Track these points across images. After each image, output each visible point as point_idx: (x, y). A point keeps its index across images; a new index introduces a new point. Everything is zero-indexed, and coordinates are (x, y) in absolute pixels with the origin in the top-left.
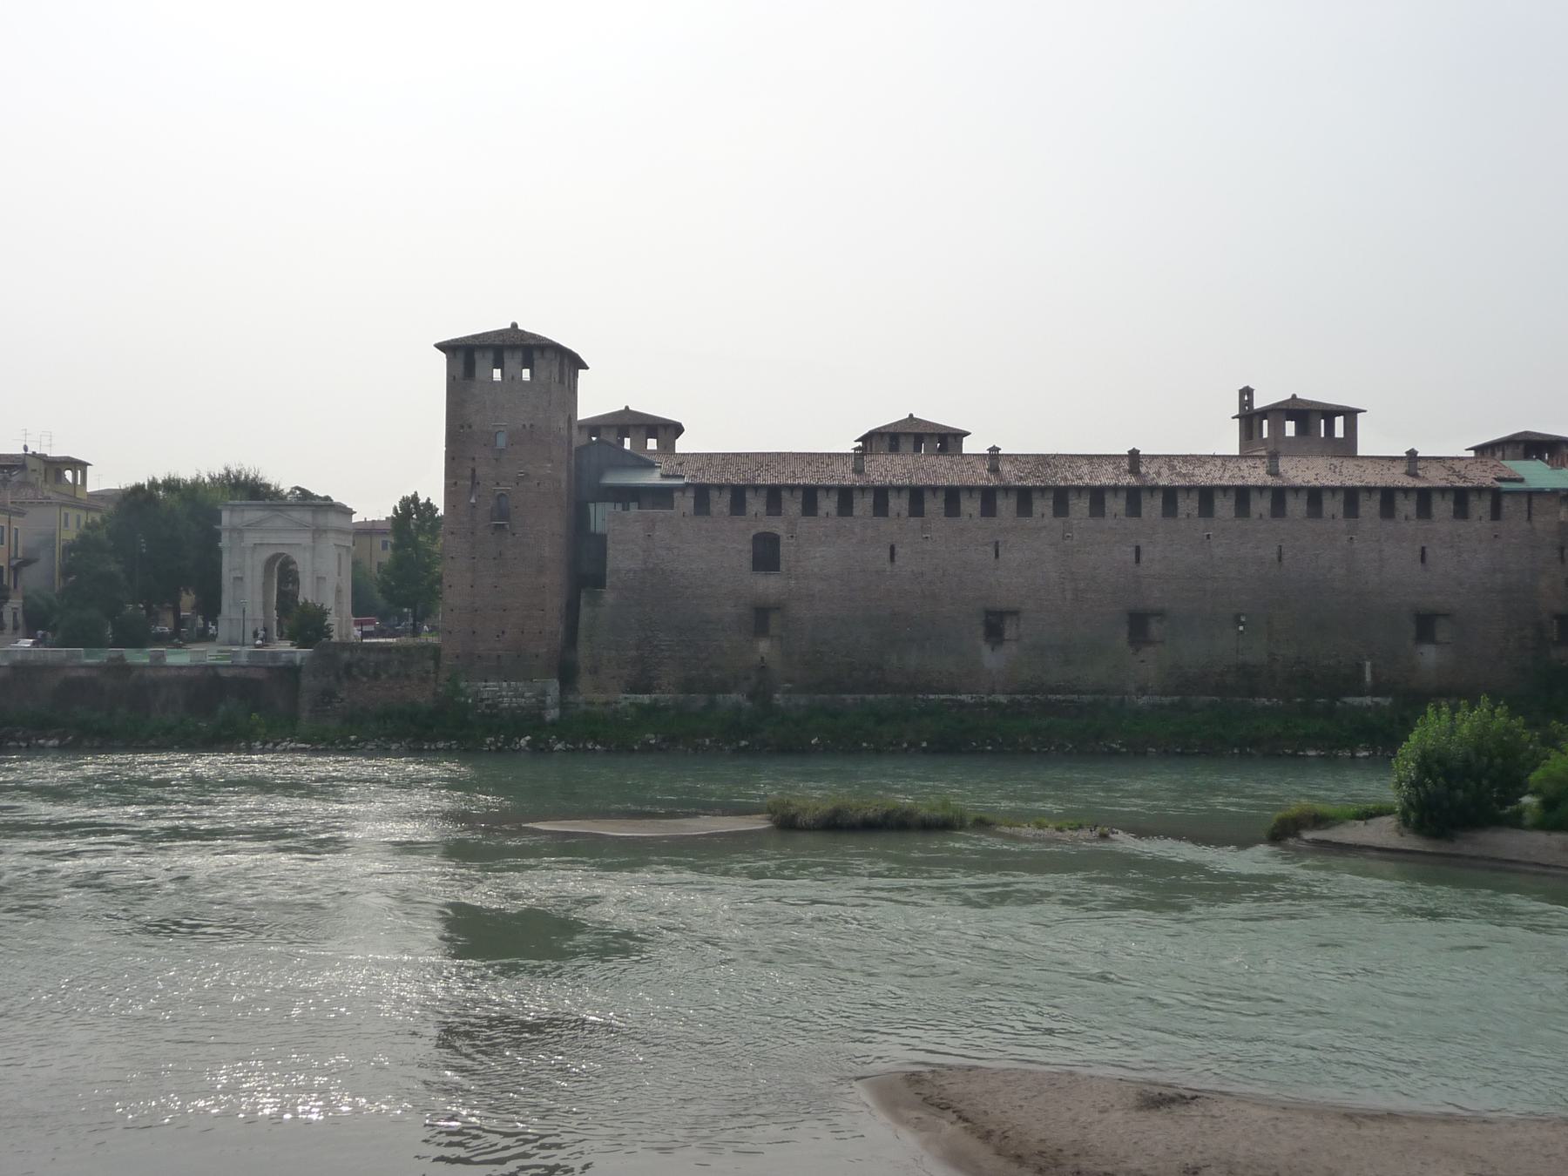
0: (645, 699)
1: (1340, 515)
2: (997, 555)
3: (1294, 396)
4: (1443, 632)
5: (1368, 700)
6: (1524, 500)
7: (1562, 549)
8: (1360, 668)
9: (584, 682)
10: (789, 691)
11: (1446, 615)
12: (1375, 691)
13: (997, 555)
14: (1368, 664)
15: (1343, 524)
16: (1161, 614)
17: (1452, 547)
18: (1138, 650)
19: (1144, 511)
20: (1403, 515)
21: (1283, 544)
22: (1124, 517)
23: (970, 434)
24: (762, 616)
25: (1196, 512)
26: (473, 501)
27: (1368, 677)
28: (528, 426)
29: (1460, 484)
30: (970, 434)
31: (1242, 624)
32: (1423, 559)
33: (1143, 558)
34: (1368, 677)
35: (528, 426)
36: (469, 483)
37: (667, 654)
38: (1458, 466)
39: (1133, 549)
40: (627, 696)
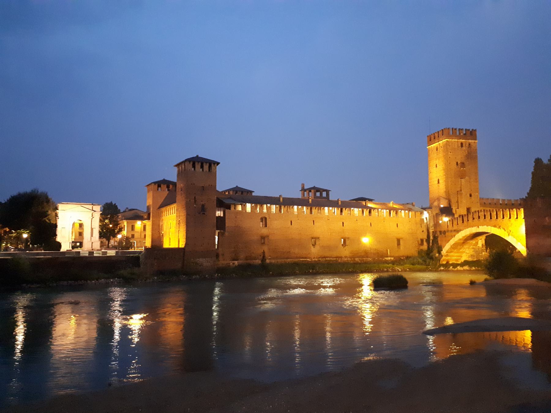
0: (236, 263)
2: (314, 224)
5: (389, 258)
8: (387, 250)
9: (221, 258)
10: (270, 259)
13: (314, 224)
14: (389, 250)
16: (348, 238)
23: (254, 192)
24: (263, 239)
26: (195, 206)
28: (210, 185)
30: (254, 192)
32: (397, 227)
35: (210, 185)
36: (194, 201)
37: (241, 250)
39: (342, 223)
40: (232, 261)
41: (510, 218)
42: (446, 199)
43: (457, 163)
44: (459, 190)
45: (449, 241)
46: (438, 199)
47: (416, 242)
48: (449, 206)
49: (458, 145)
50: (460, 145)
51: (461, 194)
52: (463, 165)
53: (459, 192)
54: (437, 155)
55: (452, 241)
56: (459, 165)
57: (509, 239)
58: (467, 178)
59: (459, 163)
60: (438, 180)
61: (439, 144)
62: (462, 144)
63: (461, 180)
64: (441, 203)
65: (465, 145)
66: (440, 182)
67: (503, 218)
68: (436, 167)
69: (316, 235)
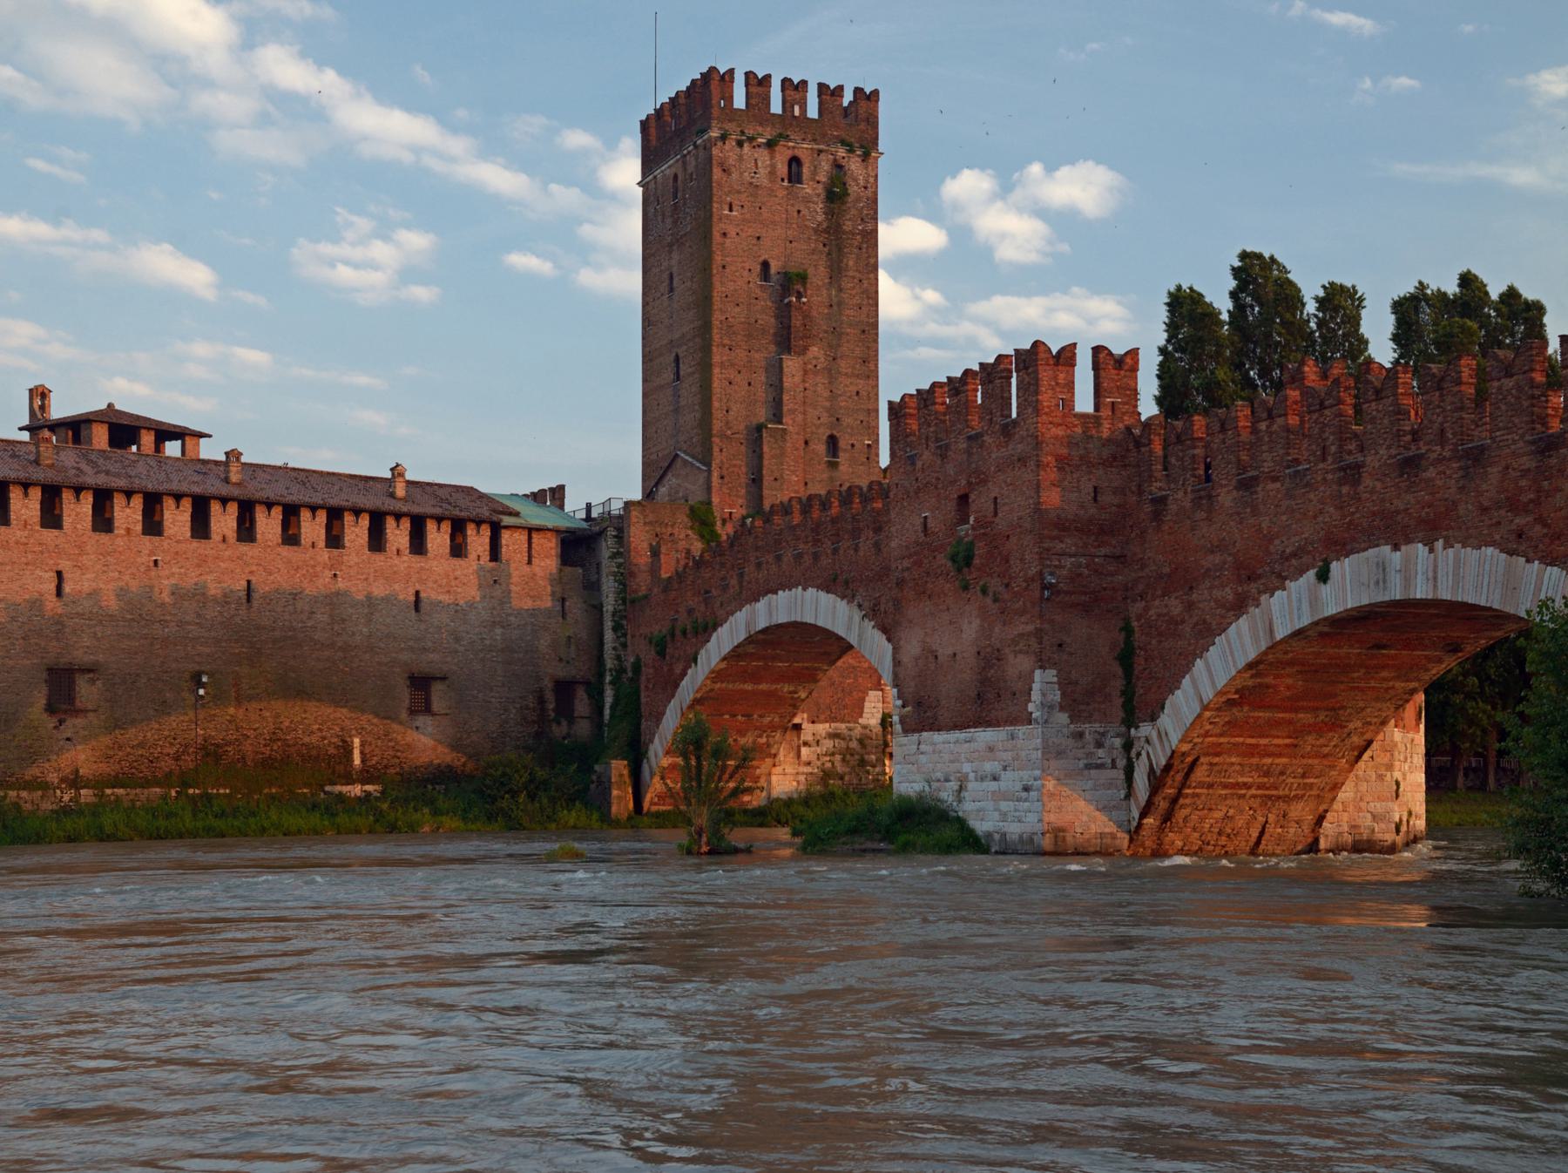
1: (322, 544)
3: (110, 406)
4: (439, 697)
6: (524, 537)
7: (563, 600)
11: (443, 679)
12: (366, 776)
14: (357, 741)
15: (325, 555)
17: (449, 592)
18: (61, 722)
19: (67, 521)
20: (394, 549)
21: (253, 579)
22: (38, 528)
25: (139, 528)
27: (357, 761)
29: (457, 512)
31: (200, 684)
33: (67, 588)
34: (357, 761)
38: (440, 492)
43: (765, 265)
47: (531, 701)
49: (773, 166)
50: (782, 169)
54: (675, 222)
56: (774, 278)
58: (814, 350)
59: (773, 270)
65: (814, 172)
68: (671, 290)
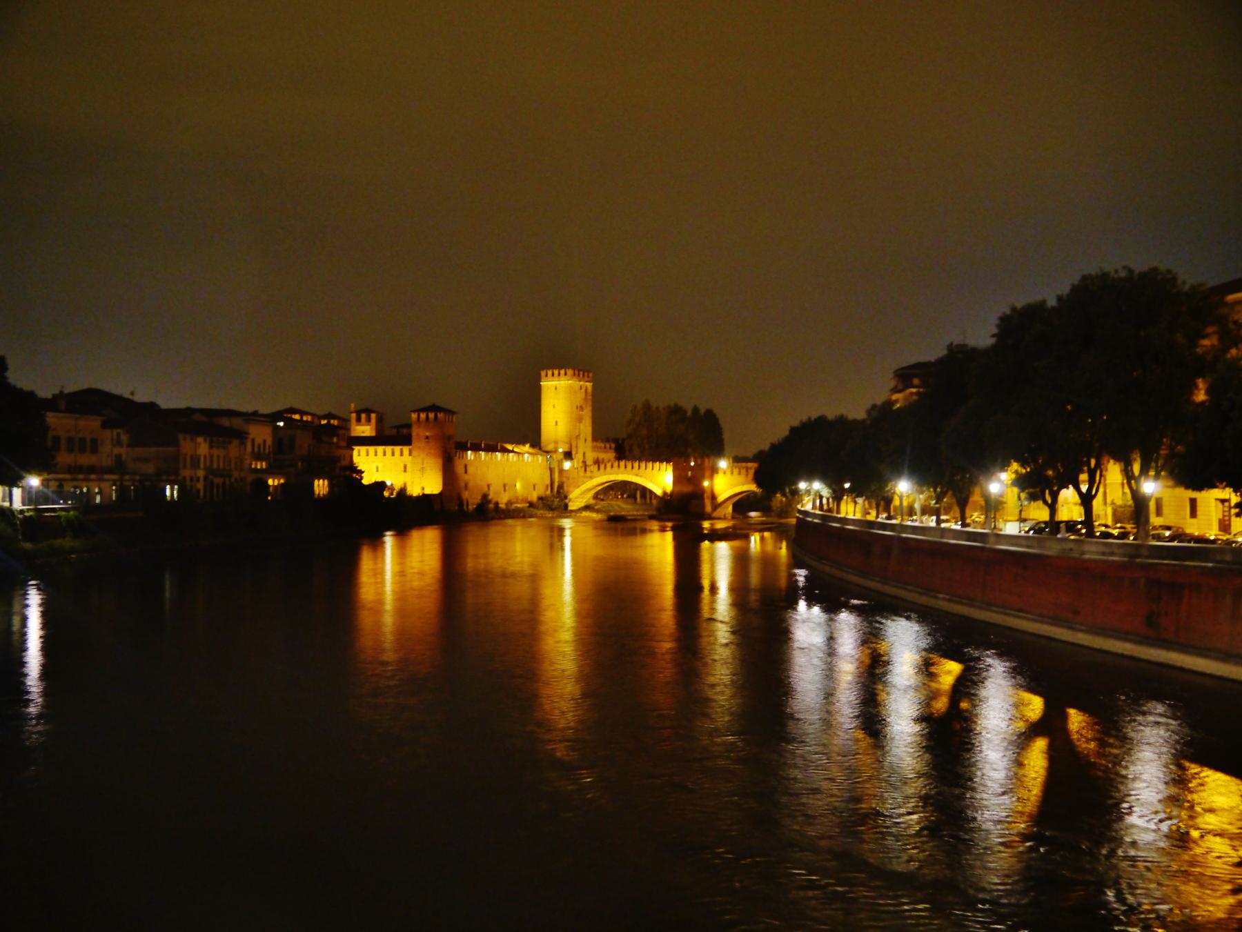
41: (653, 469)
42: (567, 443)
44: (577, 434)
45: (579, 486)
46: (556, 443)
48: (569, 450)
51: (580, 439)
52: (581, 408)
53: (578, 436)
55: (584, 488)
57: (650, 486)
60: (556, 423)
61: (560, 384)
62: (581, 387)
63: (580, 426)
64: (559, 446)
66: (558, 424)
67: (646, 468)
69: (490, 483)
